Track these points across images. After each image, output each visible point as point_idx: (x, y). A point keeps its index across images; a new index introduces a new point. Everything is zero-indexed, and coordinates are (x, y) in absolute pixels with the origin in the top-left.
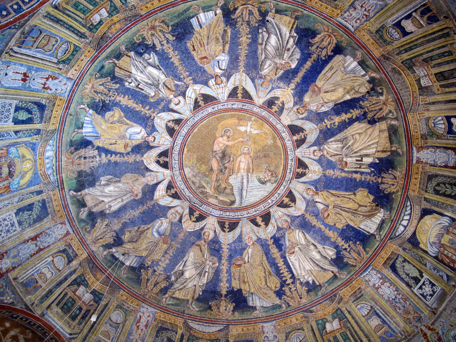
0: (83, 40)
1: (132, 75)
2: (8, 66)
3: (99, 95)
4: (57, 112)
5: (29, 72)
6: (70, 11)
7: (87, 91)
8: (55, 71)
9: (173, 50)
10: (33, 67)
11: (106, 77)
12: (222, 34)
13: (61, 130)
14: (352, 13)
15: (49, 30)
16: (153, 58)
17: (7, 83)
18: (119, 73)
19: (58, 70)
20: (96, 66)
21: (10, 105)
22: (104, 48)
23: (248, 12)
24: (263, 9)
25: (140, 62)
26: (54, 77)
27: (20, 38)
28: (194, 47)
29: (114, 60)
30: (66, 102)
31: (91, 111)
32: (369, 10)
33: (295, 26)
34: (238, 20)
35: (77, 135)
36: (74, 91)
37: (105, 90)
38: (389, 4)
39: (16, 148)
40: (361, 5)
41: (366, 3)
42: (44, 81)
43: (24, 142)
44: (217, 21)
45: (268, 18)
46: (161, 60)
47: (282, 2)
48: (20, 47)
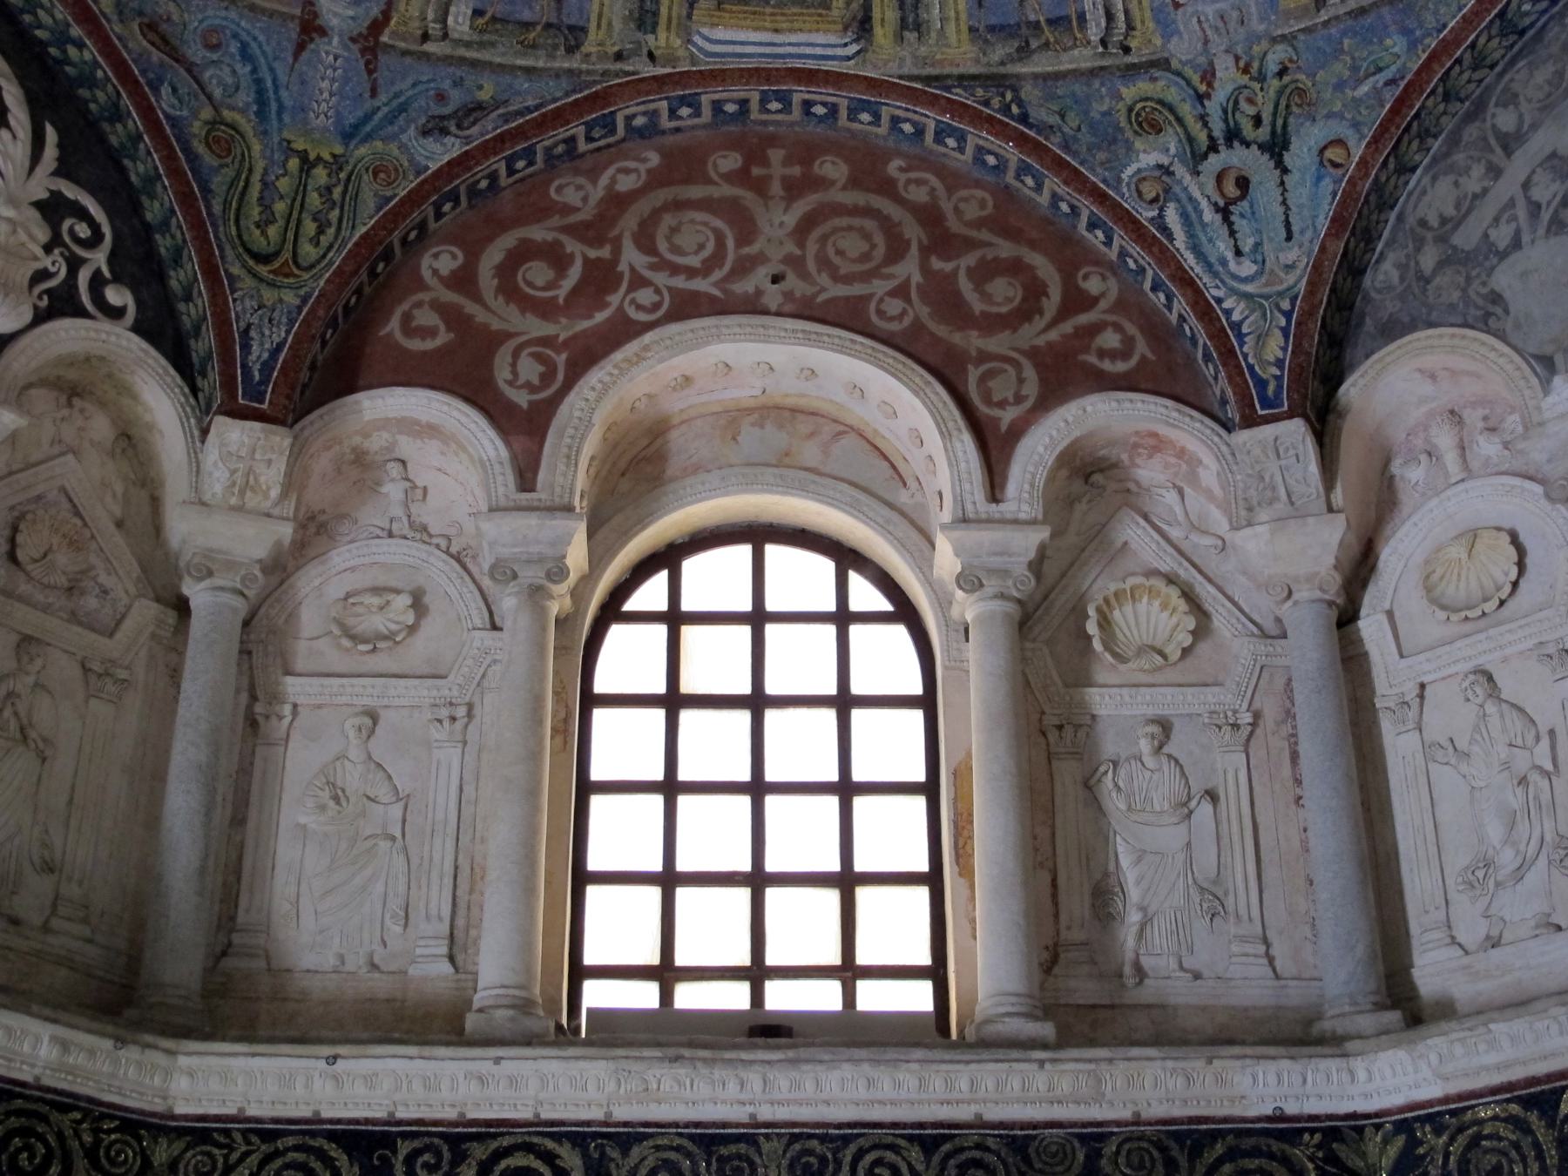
27: (1047, 44)
48: (1082, 17)
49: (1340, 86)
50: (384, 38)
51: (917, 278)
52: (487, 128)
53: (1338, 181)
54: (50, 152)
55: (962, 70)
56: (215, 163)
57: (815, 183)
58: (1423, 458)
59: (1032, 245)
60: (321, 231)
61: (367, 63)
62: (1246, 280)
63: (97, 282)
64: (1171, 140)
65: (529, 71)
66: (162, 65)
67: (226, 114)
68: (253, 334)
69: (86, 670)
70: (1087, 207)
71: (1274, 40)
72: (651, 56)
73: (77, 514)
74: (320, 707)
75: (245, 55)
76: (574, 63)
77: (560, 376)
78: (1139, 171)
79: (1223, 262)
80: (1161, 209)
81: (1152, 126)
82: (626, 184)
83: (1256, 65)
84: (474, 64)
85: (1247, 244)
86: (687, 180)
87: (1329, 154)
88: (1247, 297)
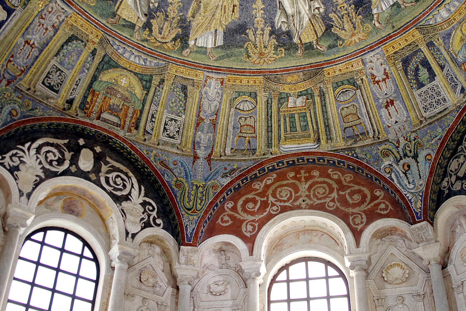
0: (324, 90)
1: (310, 16)
2: (389, 127)
3: (354, 20)
4: (400, 43)
5: (383, 105)
6: (313, 127)
7: (360, 36)
8: (367, 82)
9: (256, 18)
10: (376, 106)
11: (334, 35)
12: (198, 14)
13: (415, 23)
14: (56, 20)
15: (339, 125)
16: (280, 21)
17: (404, 115)
18: (320, 28)
19: (364, 82)
20: (334, 54)
21: (420, 95)
22: (315, 66)
23: (163, 33)
24: (147, 32)
25: (294, 24)
26: (372, 79)
28: (233, 9)
29: (315, 46)
30: (385, 44)
31: (375, 11)
32: (39, 26)
33: (118, 5)
34: (176, 25)
35: (406, 1)
36: (371, 48)
37: (345, 20)
38: (21, 37)
39: (457, 55)
40: (48, 31)
41: (43, 34)
42: (382, 84)
43: (448, 52)
44: (197, 31)
45: (144, 19)
46: (273, 14)
47: (126, 37)
49: (428, 141)
50: (212, 157)
51: (336, 197)
52: (236, 174)
53: (430, 164)
54: (143, 192)
55: (342, 148)
56: (178, 189)
57: (312, 177)
58: (459, 226)
59: (363, 186)
60: (201, 202)
61: (209, 163)
62: (412, 189)
63: (154, 219)
64: (391, 158)
65: (244, 160)
66: (165, 170)
67: (179, 178)
68: (188, 227)
69: (158, 304)
70: (374, 176)
71: (412, 132)
72: (271, 153)
73: (154, 270)
74: (209, 308)
75: (182, 165)
76: (254, 157)
77: (257, 229)
78: (385, 166)
79: (406, 185)
80: (391, 174)
81: (387, 155)
82: (269, 182)
83: (408, 138)
84: (232, 160)
85: (411, 181)
86: (283, 180)
87: (427, 157)
88: (412, 193)
